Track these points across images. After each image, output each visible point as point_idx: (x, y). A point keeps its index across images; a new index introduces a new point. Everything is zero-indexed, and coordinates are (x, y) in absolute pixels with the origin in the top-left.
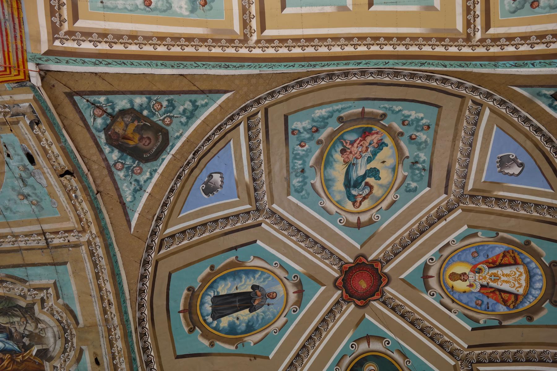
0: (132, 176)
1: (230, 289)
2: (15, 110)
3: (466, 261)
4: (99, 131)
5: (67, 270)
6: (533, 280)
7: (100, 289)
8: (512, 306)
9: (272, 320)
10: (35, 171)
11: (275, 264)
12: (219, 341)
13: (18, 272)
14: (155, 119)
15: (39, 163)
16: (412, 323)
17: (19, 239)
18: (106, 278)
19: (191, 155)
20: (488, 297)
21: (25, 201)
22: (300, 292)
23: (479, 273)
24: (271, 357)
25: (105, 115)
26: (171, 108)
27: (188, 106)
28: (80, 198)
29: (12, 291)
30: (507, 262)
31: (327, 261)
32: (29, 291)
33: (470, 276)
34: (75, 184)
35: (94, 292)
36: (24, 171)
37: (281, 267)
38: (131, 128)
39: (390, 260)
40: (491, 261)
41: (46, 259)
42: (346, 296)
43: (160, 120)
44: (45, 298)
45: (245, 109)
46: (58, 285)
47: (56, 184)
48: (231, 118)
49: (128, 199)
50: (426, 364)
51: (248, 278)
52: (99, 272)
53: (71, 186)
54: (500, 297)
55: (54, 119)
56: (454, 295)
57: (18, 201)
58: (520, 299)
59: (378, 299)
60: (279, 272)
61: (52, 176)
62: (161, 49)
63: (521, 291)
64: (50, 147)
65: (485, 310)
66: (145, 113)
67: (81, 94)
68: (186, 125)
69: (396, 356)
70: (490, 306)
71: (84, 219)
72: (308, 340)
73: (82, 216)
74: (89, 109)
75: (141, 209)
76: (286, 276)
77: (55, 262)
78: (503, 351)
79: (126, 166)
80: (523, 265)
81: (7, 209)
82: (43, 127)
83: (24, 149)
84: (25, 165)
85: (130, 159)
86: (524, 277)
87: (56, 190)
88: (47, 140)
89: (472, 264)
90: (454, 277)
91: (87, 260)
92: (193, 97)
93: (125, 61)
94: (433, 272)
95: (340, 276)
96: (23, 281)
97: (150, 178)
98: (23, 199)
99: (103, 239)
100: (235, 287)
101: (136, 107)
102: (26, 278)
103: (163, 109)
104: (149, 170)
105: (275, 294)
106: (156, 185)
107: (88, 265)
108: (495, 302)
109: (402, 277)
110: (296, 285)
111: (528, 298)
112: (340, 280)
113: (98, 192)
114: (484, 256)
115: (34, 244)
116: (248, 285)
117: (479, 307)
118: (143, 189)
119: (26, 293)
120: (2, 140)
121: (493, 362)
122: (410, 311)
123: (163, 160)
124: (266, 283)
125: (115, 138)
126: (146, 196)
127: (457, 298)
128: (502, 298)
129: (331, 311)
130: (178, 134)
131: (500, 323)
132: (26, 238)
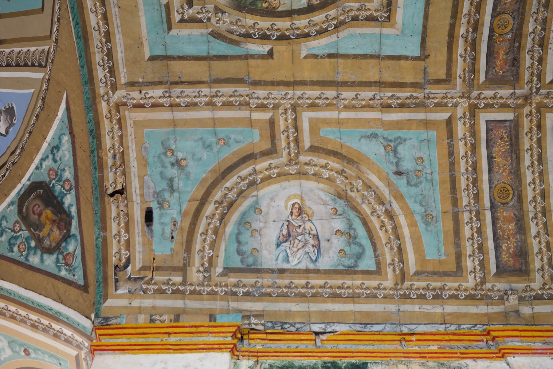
0: (58, 169)
2: (137, 285)
4: (74, 235)
5: (151, 49)
7: (105, 17)
10: (152, 199)
13: (220, 48)
14: (26, 233)
15: (141, 210)
17: (207, 99)
18: (95, 34)
21: (180, 155)
25: (65, 253)
26: (12, 242)
28: (110, 155)
29: (234, 21)
32: (209, 19)
34: (111, 175)
35: (114, 12)
36: (164, 200)
38: (46, 231)
41: (177, 67)
43: (23, 230)
44: (186, 7)
46: (165, 26)
47: (133, 178)
49: (66, 139)
52: (106, 42)
57: (189, 157)
61: (133, 190)
64: (119, 232)
66: (33, 244)
67: (78, 287)
71: (114, 122)
73: (116, 127)
74: (75, 266)
75: (55, 122)
77: (165, 62)
79: (61, 183)
81: (209, 146)
83: (151, 231)
84: (160, 209)
85: (55, 191)
87: (136, 169)
88: (119, 241)
91: (120, 62)
93: (38, 307)
96: (216, 35)
97: (43, 160)
98: (182, 159)
99: (95, 91)
101: (39, 252)
102: (211, 38)
104: (42, 171)
106: (38, 149)
107: (120, 54)
115: (189, 90)
118: (50, 148)
119: (214, 15)
120: (173, 245)
123: (29, 180)
125: (62, 223)
126: (49, 138)
130: (12, 208)
132: (196, 100)
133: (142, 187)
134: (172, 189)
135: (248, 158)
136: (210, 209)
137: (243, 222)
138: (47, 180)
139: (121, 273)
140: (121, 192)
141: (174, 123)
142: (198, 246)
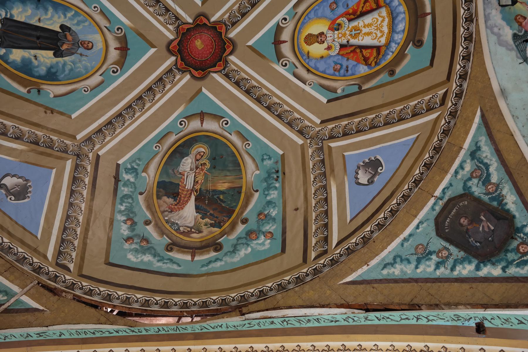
1: (30, 17)
3: (324, 17)
6: (396, 22)
8: (373, 64)
9: (83, 75)
11: (95, 7)
12: (5, 74)
16: (258, 101)
20: (348, 60)
22: (124, 49)
23: (338, 30)
24: (74, 116)
30: (369, 8)
31: (160, 18)
33: (328, 35)
37: (102, 13)
39: (236, 22)
40: (351, 11)
42: (181, 64)
50: (268, 146)
51: (57, 13)
54: (361, 56)
56: (310, 63)
58: (383, 50)
59: (220, 71)
60: (98, 18)
63: (383, 41)
65: (344, 76)
69: (234, 138)
70: (349, 69)
72: (127, 108)
76: (108, 25)
78: (360, 119)
80: (385, 6)
86: (387, 20)
89: (330, 19)
90: (311, 39)
94: (286, 36)
95: (175, 39)
100: (37, 18)
105: (90, 45)
108: (355, 63)
109: (250, 43)
110: (118, 39)
111: (391, 47)
112: (175, 43)
114: (343, 6)
116: (54, 22)
117: (337, 73)
121: (348, 134)
122: (257, 85)
124: (81, 27)
127: (313, 66)
128: (363, 56)
129: (160, 80)
131: (360, 87)
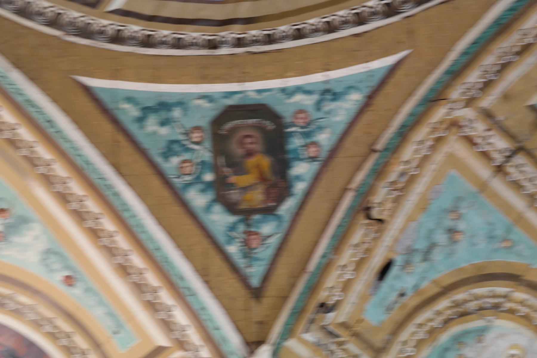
19: (224, 51)
21: (461, 226)
25: (253, 229)
27: (152, 124)
45: (85, 32)
48: (117, 38)
49: (355, 98)
53: (388, 193)
55: (302, 294)
62: (108, 225)
66: (209, 177)
68: (181, 103)
73: (430, 143)
82: (322, 295)
92: (133, 128)
103: (187, 156)
107: (512, 76)
113: (375, 151)
123: (260, 91)
133: (403, 230)
134: (427, 255)
135: (512, 277)
136: (443, 304)
137: (458, 340)
138: (288, 119)
139: (321, 315)
140: (380, 221)
141: (483, 187)
142: (404, 335)
